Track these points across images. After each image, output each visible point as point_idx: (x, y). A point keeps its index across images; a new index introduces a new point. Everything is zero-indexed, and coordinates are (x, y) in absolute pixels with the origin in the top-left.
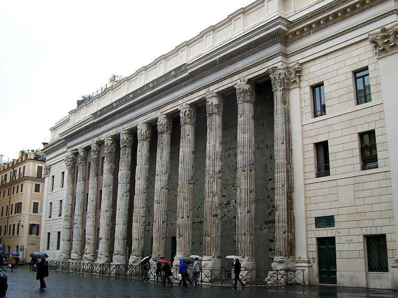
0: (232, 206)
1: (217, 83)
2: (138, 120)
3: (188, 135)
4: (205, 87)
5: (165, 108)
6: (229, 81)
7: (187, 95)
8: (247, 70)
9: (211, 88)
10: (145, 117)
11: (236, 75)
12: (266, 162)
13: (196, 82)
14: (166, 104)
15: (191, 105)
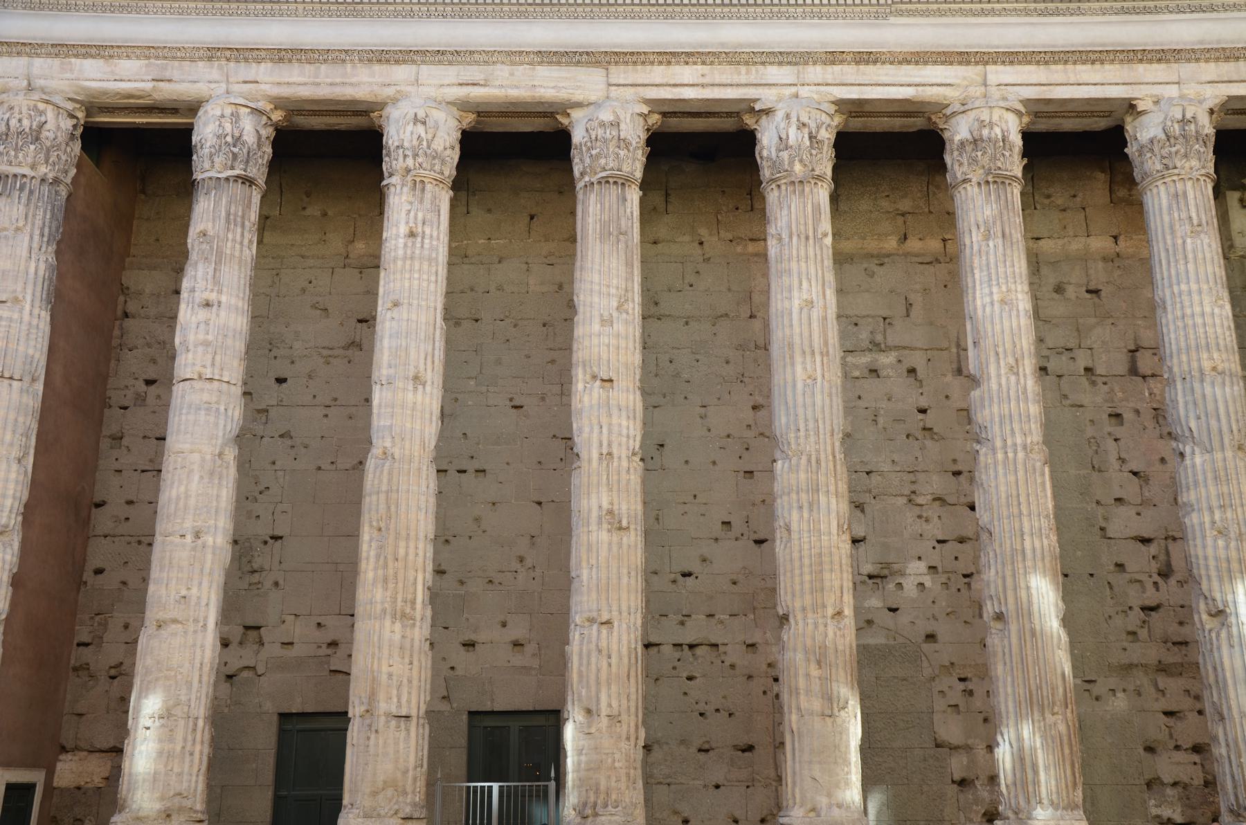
0: (909, 584)
1: (1038, 63)
2: (401, 73)
3: (826, 235)
4: (963, 58)
5: (658, 73)
6: (1111, 72)
7: (833, 57)
8: (1227, 59)
9: (999, 74)
10: (474, 73)
11: (1159, 61)
12: (1090, 431)
13: (892, 20)
14: (669, 57)
15: (843, 106)
